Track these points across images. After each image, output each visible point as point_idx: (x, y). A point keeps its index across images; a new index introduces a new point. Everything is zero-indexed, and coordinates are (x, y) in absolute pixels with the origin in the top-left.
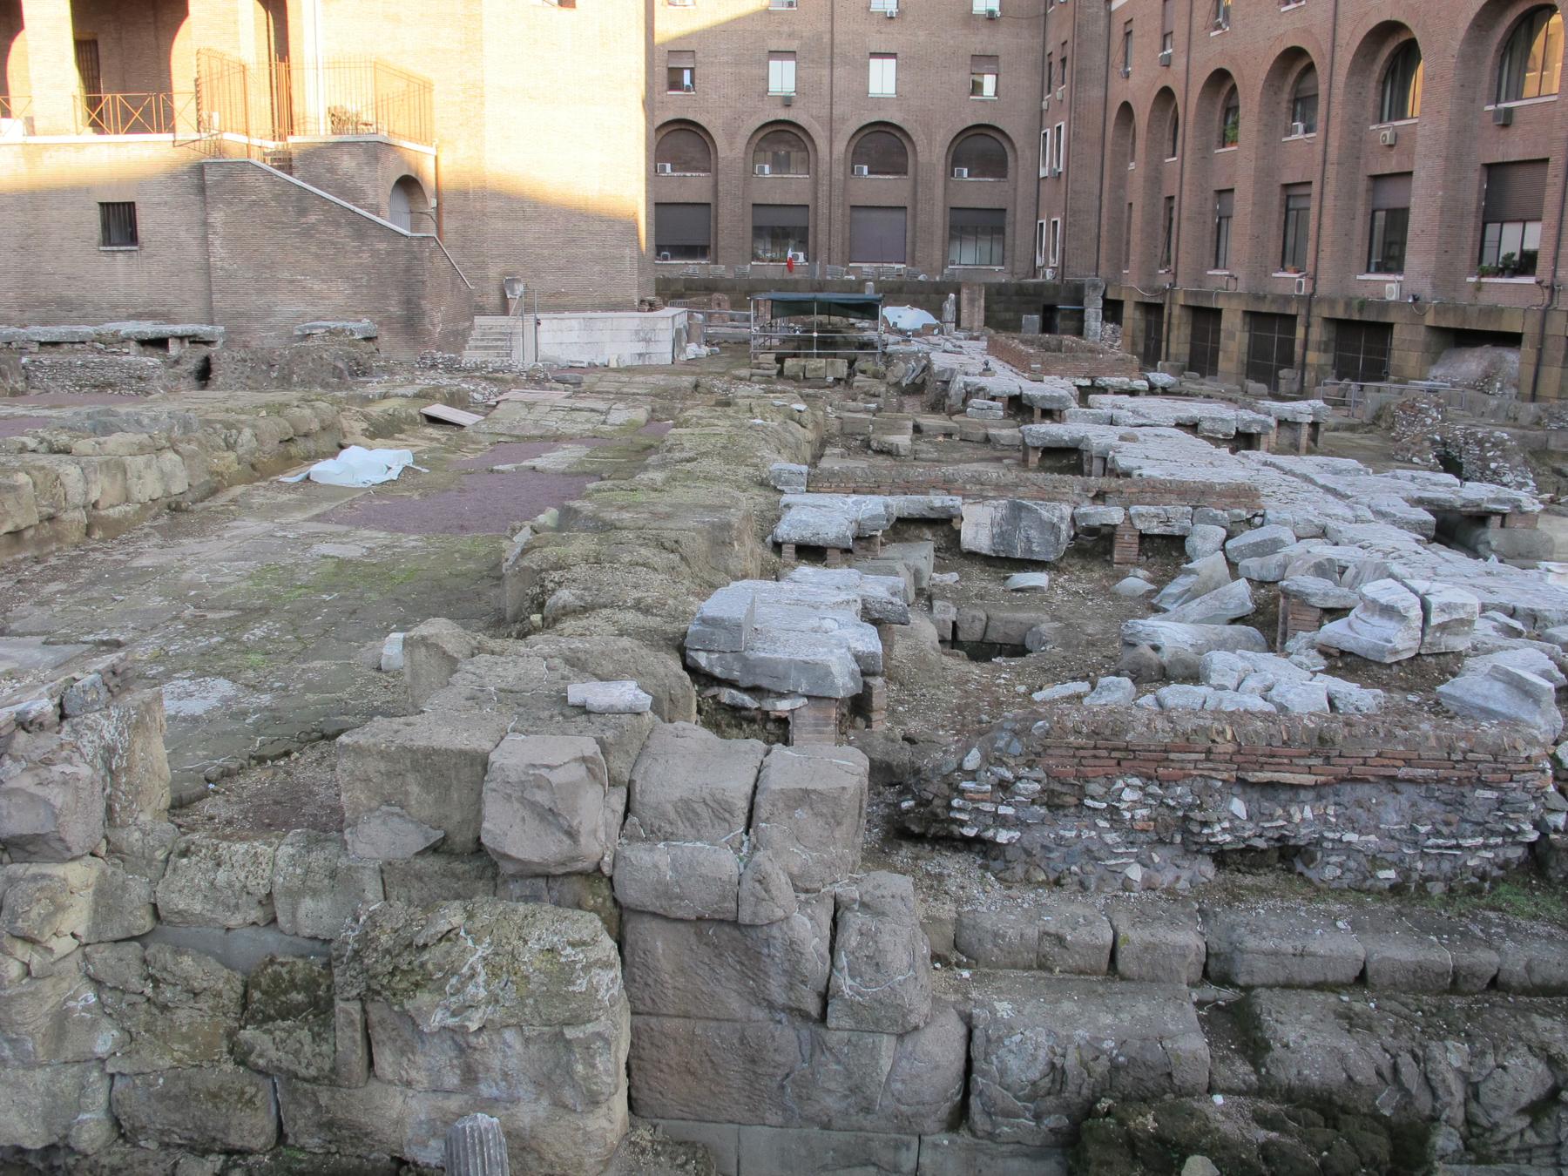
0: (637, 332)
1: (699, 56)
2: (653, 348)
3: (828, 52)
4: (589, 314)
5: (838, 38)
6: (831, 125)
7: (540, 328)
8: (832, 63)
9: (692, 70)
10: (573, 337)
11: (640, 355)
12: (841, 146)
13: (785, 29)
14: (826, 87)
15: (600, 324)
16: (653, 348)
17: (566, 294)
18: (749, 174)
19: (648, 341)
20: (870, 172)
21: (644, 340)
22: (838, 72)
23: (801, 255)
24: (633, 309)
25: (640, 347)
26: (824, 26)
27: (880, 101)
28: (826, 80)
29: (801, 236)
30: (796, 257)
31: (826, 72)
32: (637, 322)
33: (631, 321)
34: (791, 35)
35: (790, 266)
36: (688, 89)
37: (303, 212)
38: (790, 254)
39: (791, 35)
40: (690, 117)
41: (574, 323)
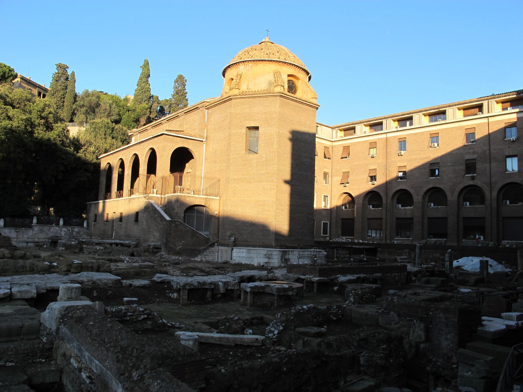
0: (265, 255)
1: (441, 163)
2: (271, 261)
3: (488, 158)
4: (250, 248)
5: (492, 152)
6: (491, 185)
7: (234, 251)
8: (490, 162)
9: (438, 169)
10: (244, 255)
11: (266, 263)
12: (495, 194)
13: (471, 151)
14: (488, 171)
15: (253, 251)
16: (271, 261)
17: (250, 242)
18: (459, 206)
19: (269, 258)
20: (510, 203)
21: (268, 258)
22: (492, 165)
23: (482, 238)
24: (273, 248)
25: (266, 260)
26: (486, 148)
27: (512, 174)
28: (488, 168)
29: (482, 230)
30: (480, 238)
31: (488, 165)
32: (266, 251)
33: (263, 251)
34: (474, 153)
35: (478, 242)
36: (436, 176)
37: (155, 214)
38: (477, 237)
39: (474, 153)
40: (438, 186)
41: (244, 250)
